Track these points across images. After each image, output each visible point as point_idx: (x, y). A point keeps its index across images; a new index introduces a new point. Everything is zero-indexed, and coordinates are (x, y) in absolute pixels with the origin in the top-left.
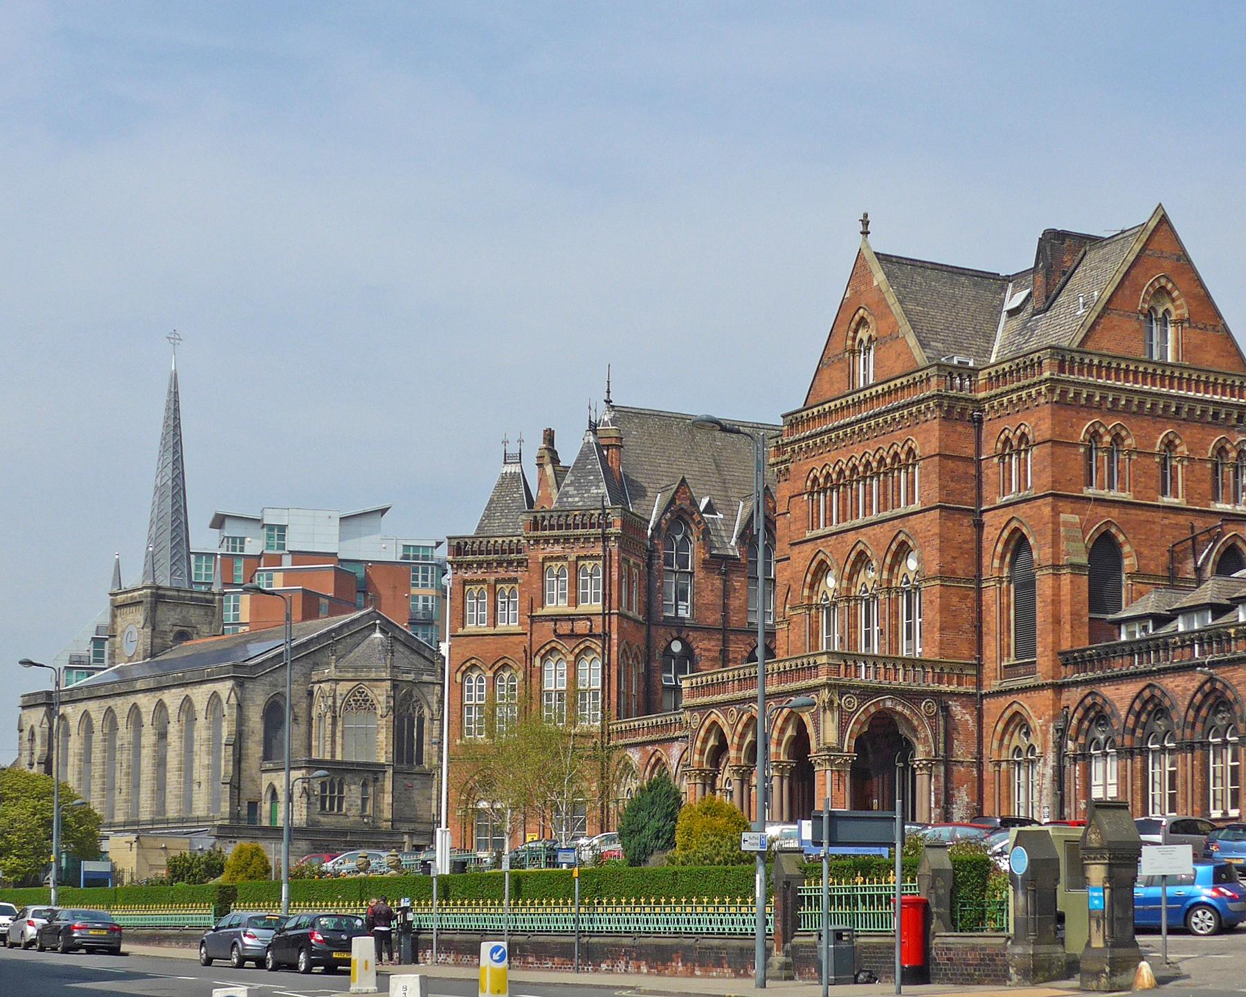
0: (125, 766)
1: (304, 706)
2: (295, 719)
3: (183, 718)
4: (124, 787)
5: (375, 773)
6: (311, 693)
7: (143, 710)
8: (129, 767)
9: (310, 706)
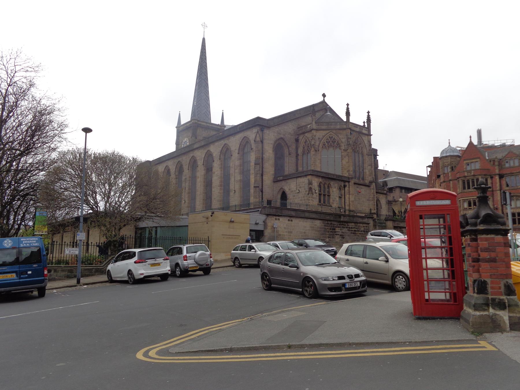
0: (187, 189)
1: (294, 147)
2: (290, 154)
3: (222, 157)
4: (186, 200)
5: (345, 181)
6: (297, 140)
7: (198, 158)
8: (189, 189)
9: (297, 149)
